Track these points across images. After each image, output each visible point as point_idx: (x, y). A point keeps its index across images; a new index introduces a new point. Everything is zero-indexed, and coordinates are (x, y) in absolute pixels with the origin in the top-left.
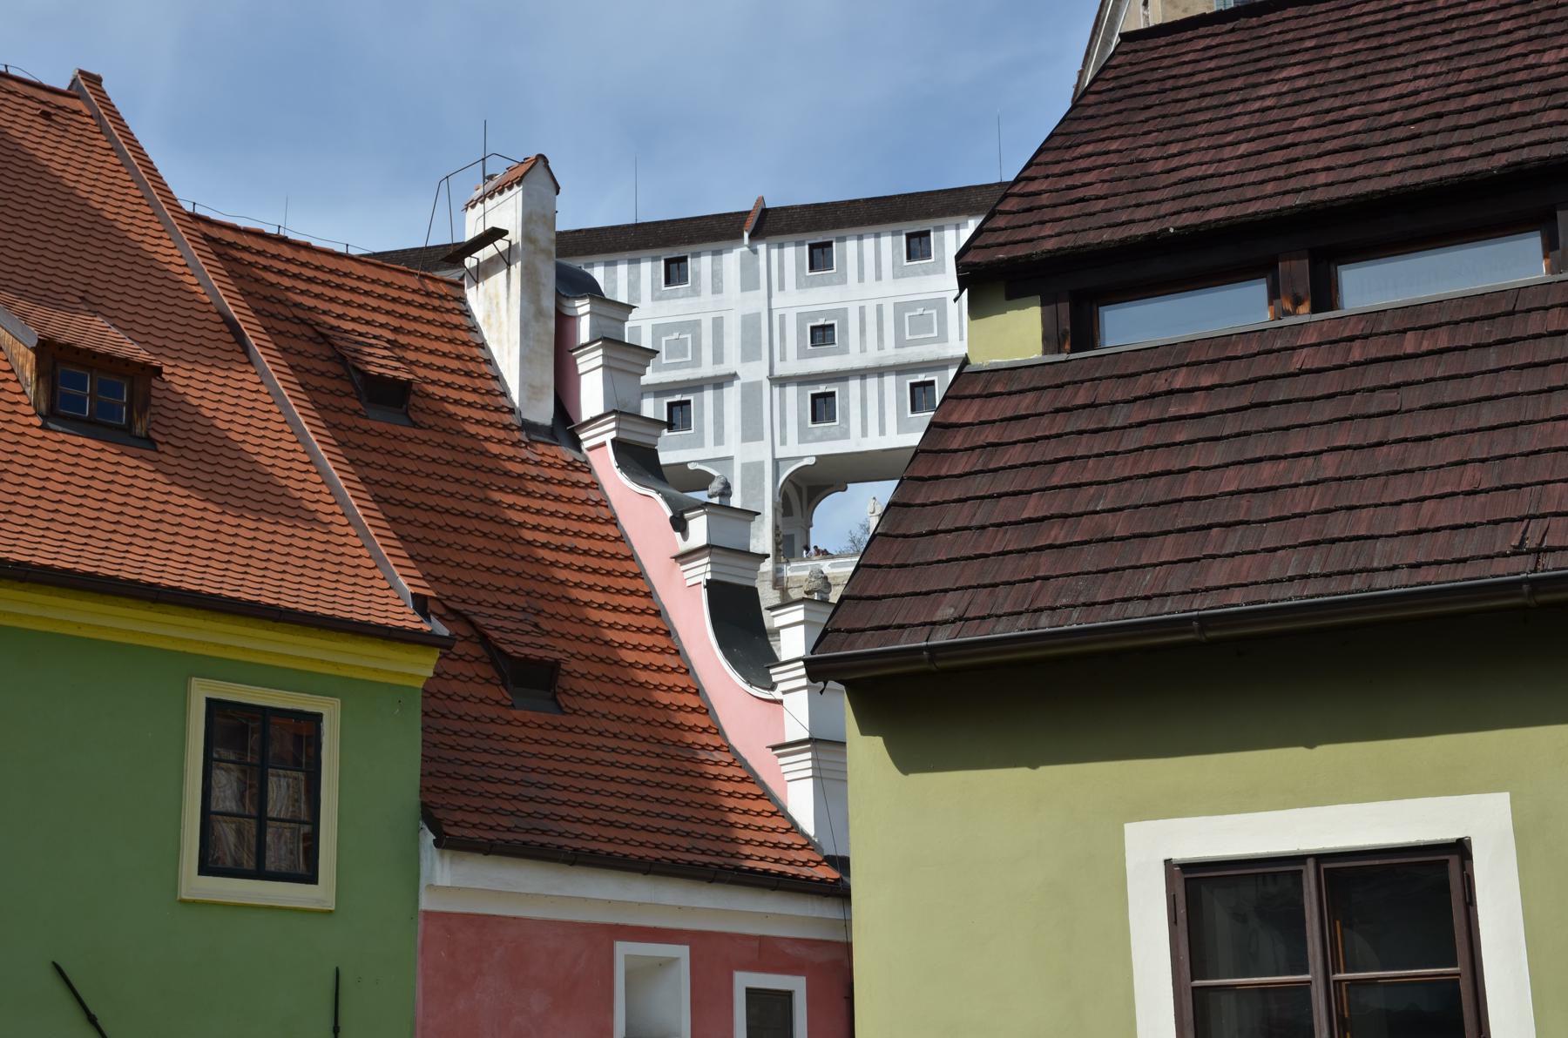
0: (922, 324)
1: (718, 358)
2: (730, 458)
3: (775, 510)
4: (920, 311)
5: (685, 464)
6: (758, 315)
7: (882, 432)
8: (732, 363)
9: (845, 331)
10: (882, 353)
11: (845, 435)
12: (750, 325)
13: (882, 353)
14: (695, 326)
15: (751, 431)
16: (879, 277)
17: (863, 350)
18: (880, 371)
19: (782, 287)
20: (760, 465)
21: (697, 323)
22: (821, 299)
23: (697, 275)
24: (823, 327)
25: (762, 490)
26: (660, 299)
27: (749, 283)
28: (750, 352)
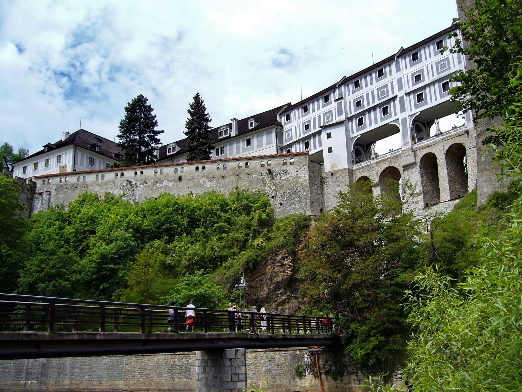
0: (443, 66)
1: (393, 93)
2: (398, 119)
3: (412, 130)
4: (442, 63)
5: (388, 124)
6: (401, 78)
7: (436, 100)
8: (396, 93)
9: (423, 75)
10: (434, 78)
11: (426, 103)
12: (400, 81)
13: (434, 78)
14: (386, 86)
15: (403, 110)
16: (430, 57)
17: (429, 79)
18: (433, 83)
19: (406, 68)
20: (406, 118)
21: (387, 85)
22: (417, 68)
23: (386, 72)
24: (418, 76)
25: (407, 125)
26: (378, 81)
27: (398, 69)
28: (400, 88)
